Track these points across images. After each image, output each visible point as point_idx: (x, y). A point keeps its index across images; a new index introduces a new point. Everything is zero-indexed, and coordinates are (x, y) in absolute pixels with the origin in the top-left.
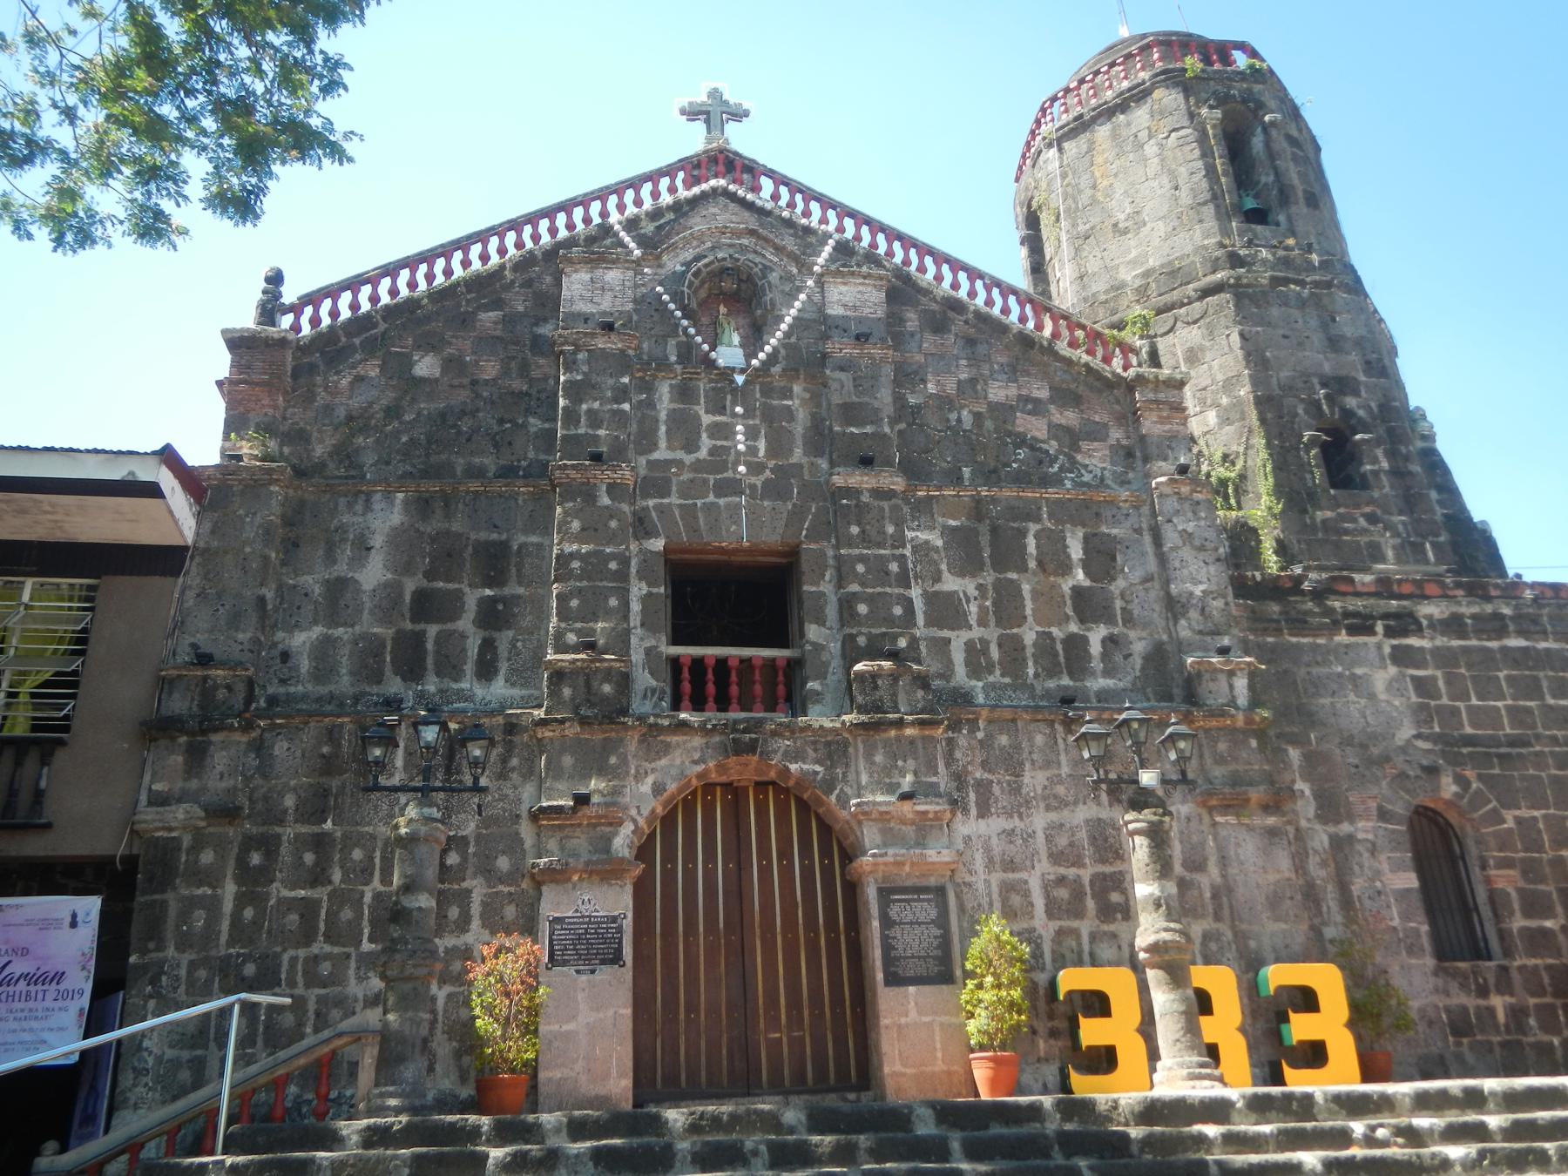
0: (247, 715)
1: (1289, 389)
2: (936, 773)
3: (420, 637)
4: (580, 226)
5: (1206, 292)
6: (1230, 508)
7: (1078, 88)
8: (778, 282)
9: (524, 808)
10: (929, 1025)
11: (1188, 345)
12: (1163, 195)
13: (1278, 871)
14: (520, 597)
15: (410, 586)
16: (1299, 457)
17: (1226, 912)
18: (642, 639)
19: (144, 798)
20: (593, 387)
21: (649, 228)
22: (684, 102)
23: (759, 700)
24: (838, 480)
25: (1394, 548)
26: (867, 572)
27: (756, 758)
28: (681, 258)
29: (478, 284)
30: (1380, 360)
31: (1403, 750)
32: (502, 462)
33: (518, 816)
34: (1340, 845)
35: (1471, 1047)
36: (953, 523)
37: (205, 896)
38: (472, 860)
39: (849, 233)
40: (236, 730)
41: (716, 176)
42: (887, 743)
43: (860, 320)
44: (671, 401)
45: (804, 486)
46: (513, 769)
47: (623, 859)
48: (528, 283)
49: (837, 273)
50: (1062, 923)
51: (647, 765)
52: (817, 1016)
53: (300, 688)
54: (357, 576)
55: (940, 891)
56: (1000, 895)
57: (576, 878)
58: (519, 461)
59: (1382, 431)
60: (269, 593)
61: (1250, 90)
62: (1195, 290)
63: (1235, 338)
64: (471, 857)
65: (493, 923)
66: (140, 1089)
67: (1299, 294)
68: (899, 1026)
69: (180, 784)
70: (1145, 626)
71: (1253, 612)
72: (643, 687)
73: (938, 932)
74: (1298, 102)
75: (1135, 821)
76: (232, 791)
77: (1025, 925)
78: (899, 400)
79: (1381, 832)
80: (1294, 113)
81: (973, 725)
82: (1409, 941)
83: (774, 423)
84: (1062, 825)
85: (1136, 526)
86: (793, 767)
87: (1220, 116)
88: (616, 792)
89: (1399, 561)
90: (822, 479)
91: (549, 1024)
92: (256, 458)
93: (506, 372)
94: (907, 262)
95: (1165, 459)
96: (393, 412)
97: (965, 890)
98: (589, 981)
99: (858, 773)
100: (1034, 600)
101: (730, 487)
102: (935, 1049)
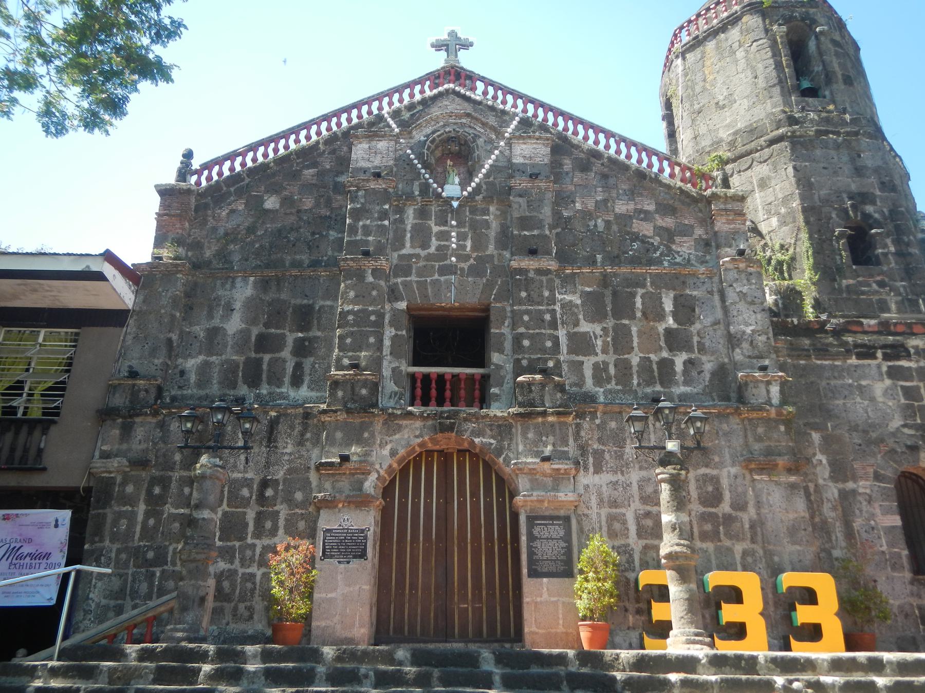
0: (155, 407)
1: (826, 201)
2: (567, 445)
3: (259, 362)
4: (365, 116)
5: (772, 142)
6: (784, 279)
7: (697, 19)
8: (483, 145)
9: (312, 463)
10: (557, 602)
11: (761, 176)
12: (747, 83)
13: (796, 512)
14: (318, 337)
15: (255, 331)
16: (832, 245)
17: (759, 538)
18: (390, 362)
19: (97, 454)
20: (367, 212)
21: (406, 115)
22: (433, 40)
23: (462, 399)
24: (514, 264)
25: (896, 303)
26: (530, 320)
27: (454, 434)
28: (424, 133)
29: (303, 153)
30: (891, 181)
31: (893, 434)
32: (313, 258)
33: (309, 468)
34: (846, 497)
37: (127, 511)
38: (280, 493)
39: (530, 113)
40: (149, 415)
41: (449, 82)
42: (536, 426)
43: (533, 166)
44: (414, 218)
45: (494, 269)
46: (307, 440)
47: (368, 495)
48: (333, 152)
49: (520, 137)
51: (388, 439)
52: (490, 596)
53: (190, 391)
54: (225, 326)
55: (567, 519)
56: (607, 522)
57: (340, 505)
58: (322, 257)
59: (891, 227)
60: (175, 337)
61: (807, 13)
62: (765, 141)
63: (790, 170)
64: (280, 491)
65: (291, 530)
66: (87, 622)
67: (835, 140)
68: (536, 603)
69: (116, 447)
70: (713, 353)
71: (791, 344)
72: (390, 391)
73: (564, 545)
74: (844, 18)
75: (662, 473)
76: (146, 451)
77: (623, 542)
78: (557, 215)
79: (876, 489)
80: (840, 25)
81: (593, 415)
82: (893, 561)
83: (478, 231)
84: (650, 479)
85: (709, 290)
86: (477, 440)
87: (785, 30)
88: (367, 454)
89: (899, 311)
90: (506, 264)
91: (320, 593)
92: (170, 258)
93: (317, 205)
94: (566, 129)
95: (730, 247)
96: (251, 230)
97: (584, 519)
98: (345, 568)
99: (517, 444)
101: (448, 270)
102: (558, 618)
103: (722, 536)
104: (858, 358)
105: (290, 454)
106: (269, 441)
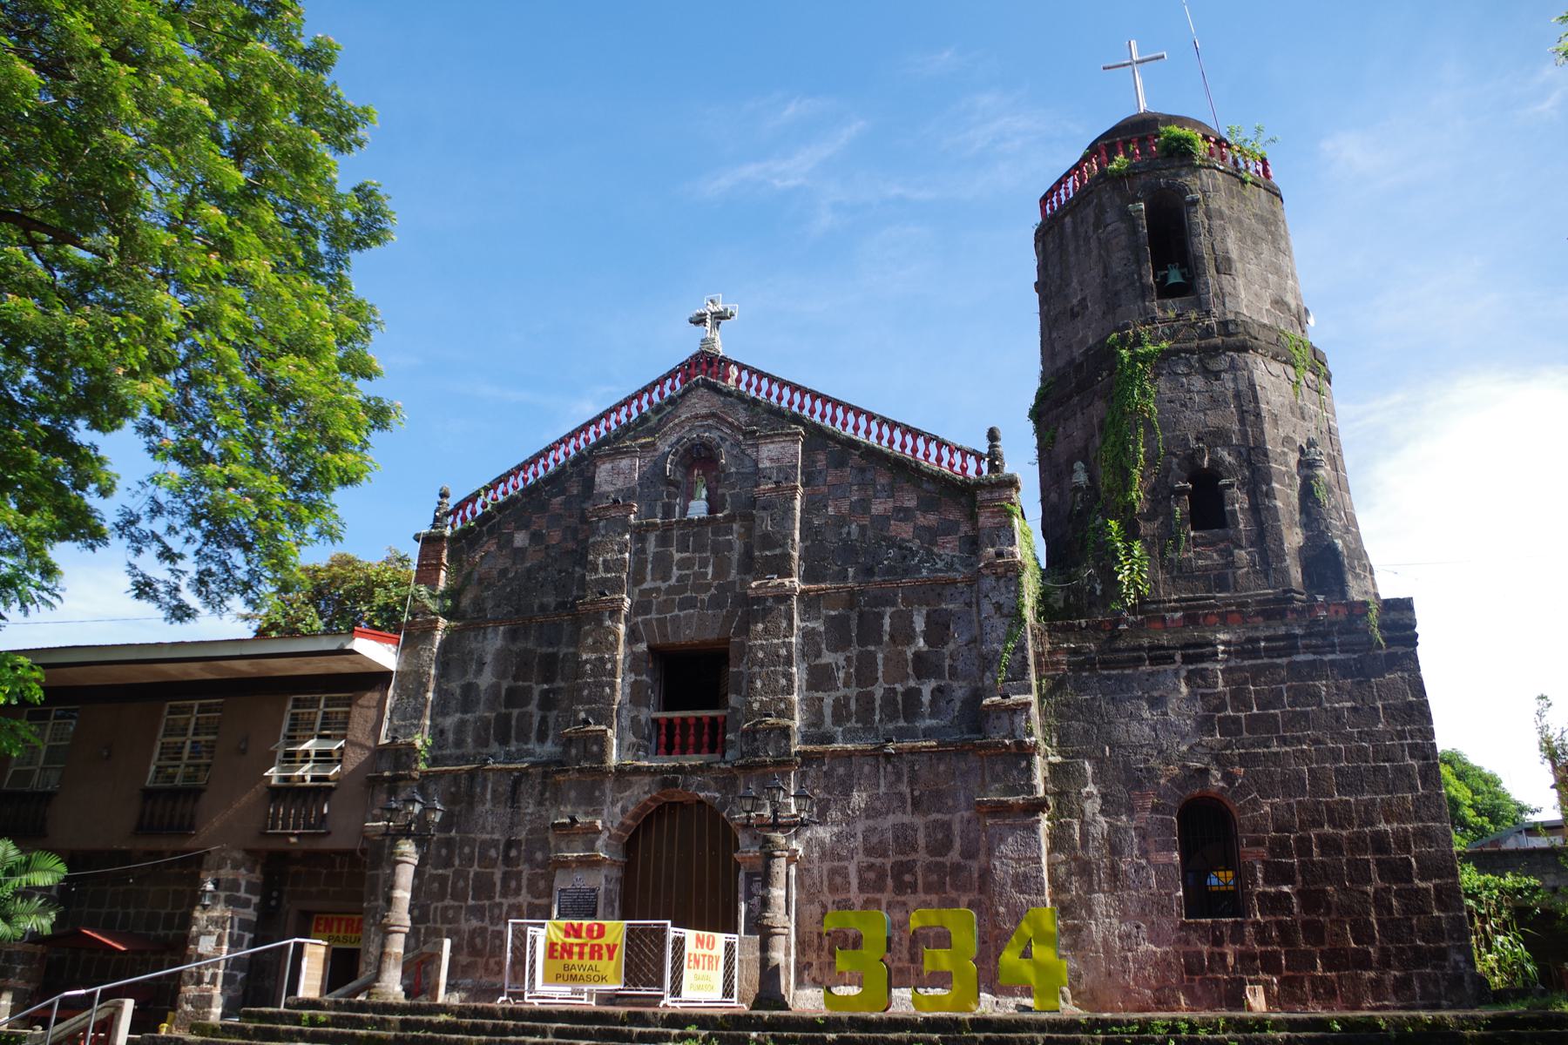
3: (508, 717)
15: (505, 685)
29: (552, 480)
35: (1201, 982)
36: (833, 613)
38: (523, 854)
44: (656, 546)
51: (619, 796)
53: (448, 752)
77: (844, 897)
103: (948, 887)
104: (1151, 664)
105: (531, 814)
106: (513, 802)
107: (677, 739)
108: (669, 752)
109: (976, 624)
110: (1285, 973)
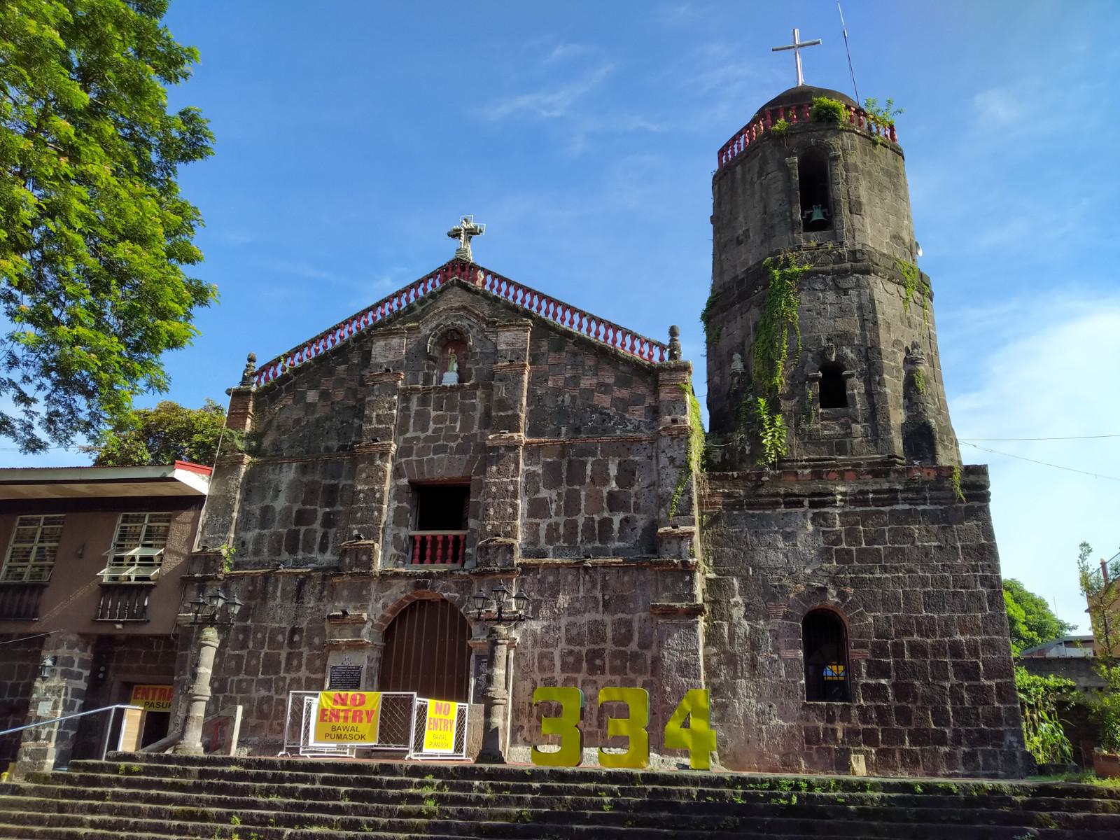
14: (340, 511)
15: (295, 508)
35: (818, 751)
36: (549, 460)
38: (304, 639)
50: (569, 675)
51: (382, 594)
77: (549, 675)
93: (346, 397)
100: (586, 500)
103: (628, 671)
104: (786, 507)
106: (298, 599)
107: (428, 552)
108: (422, 561)
109: (655, 473)
110: (882, 746)
